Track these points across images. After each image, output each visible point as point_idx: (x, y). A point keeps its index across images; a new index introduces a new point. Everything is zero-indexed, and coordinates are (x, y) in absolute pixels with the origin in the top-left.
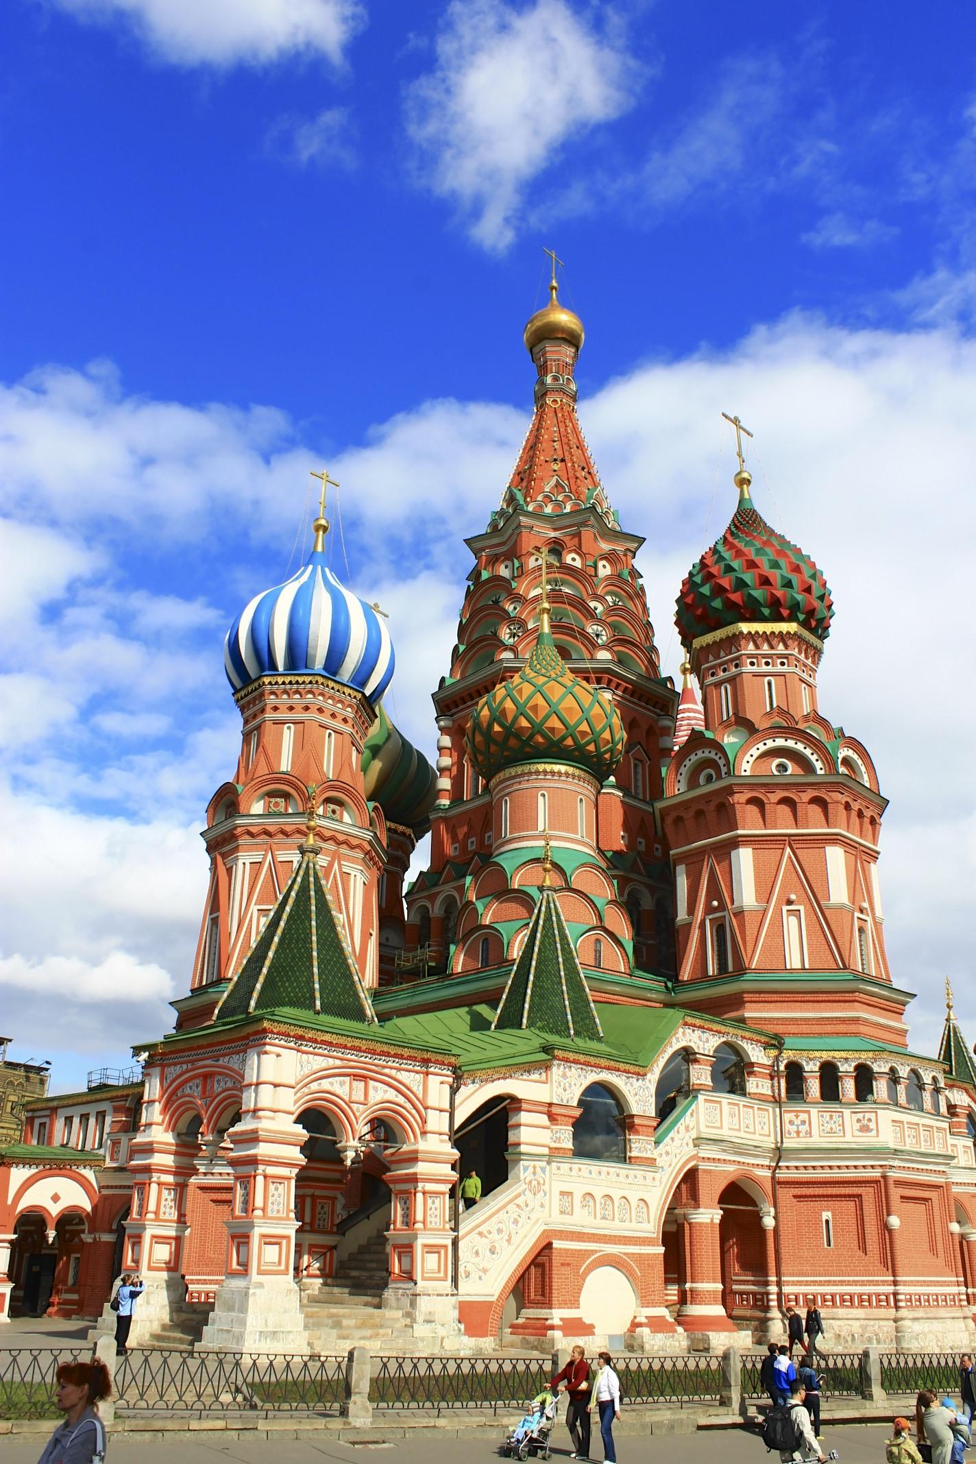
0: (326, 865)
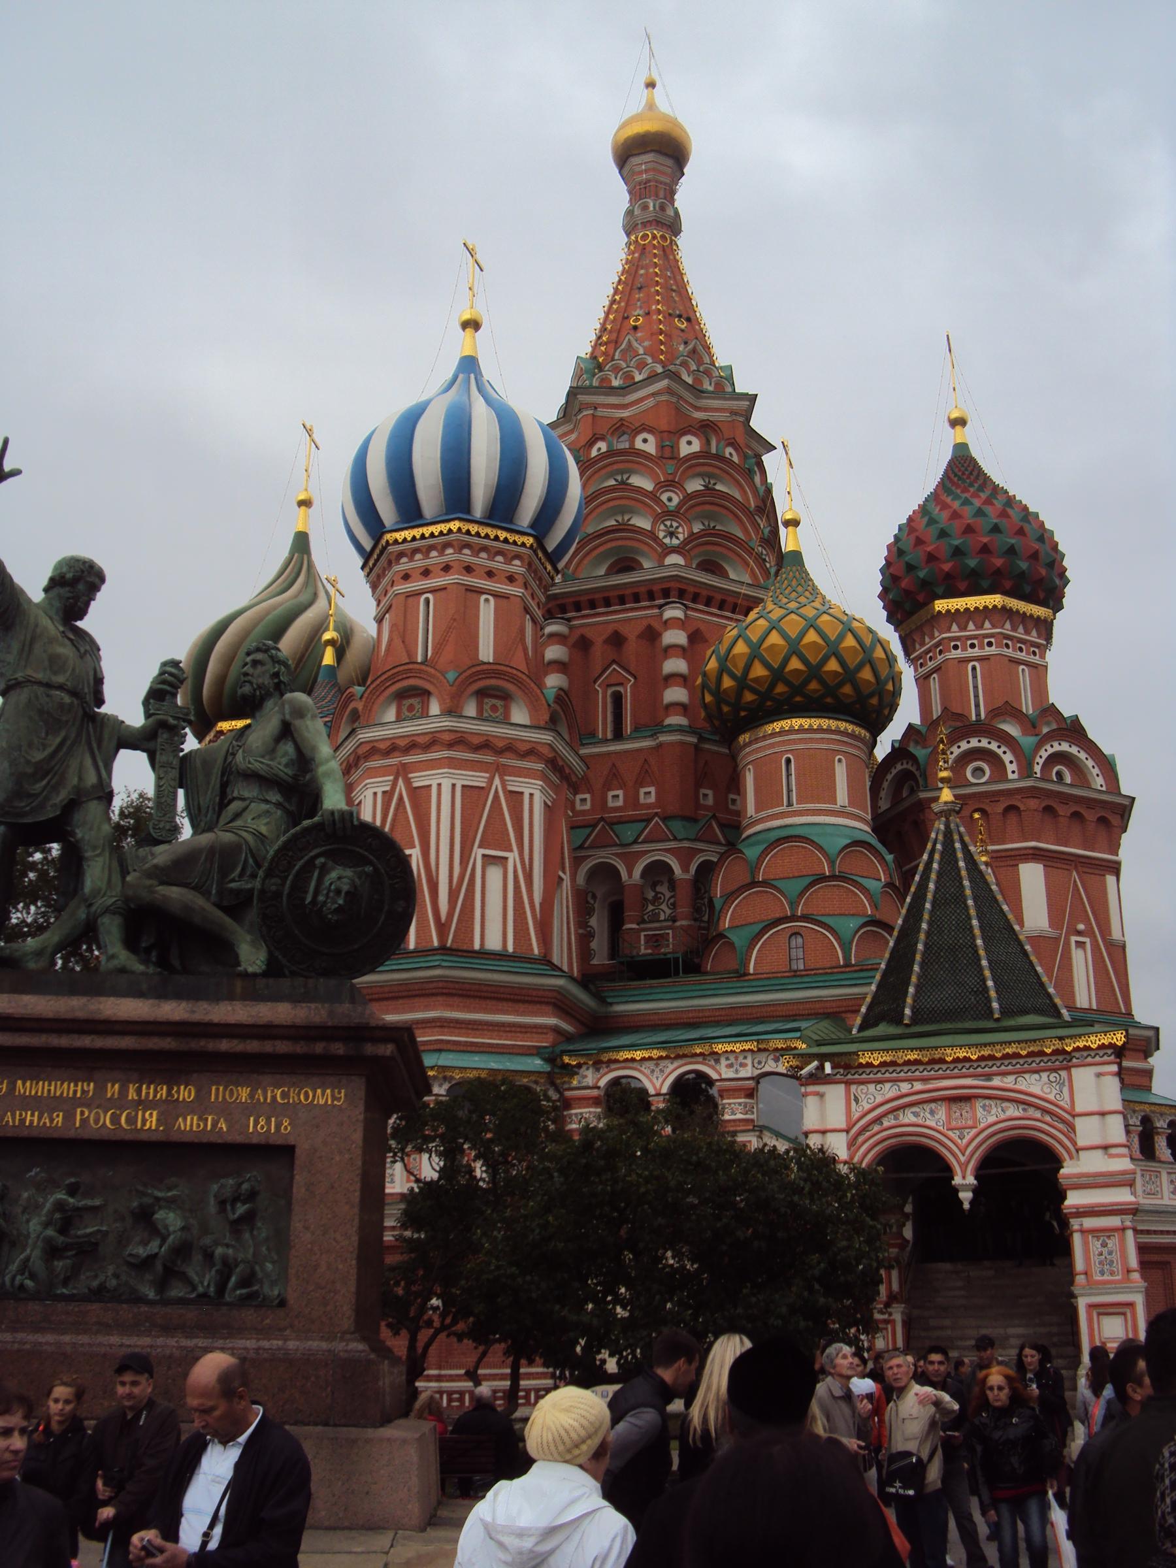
0: (550, 804)
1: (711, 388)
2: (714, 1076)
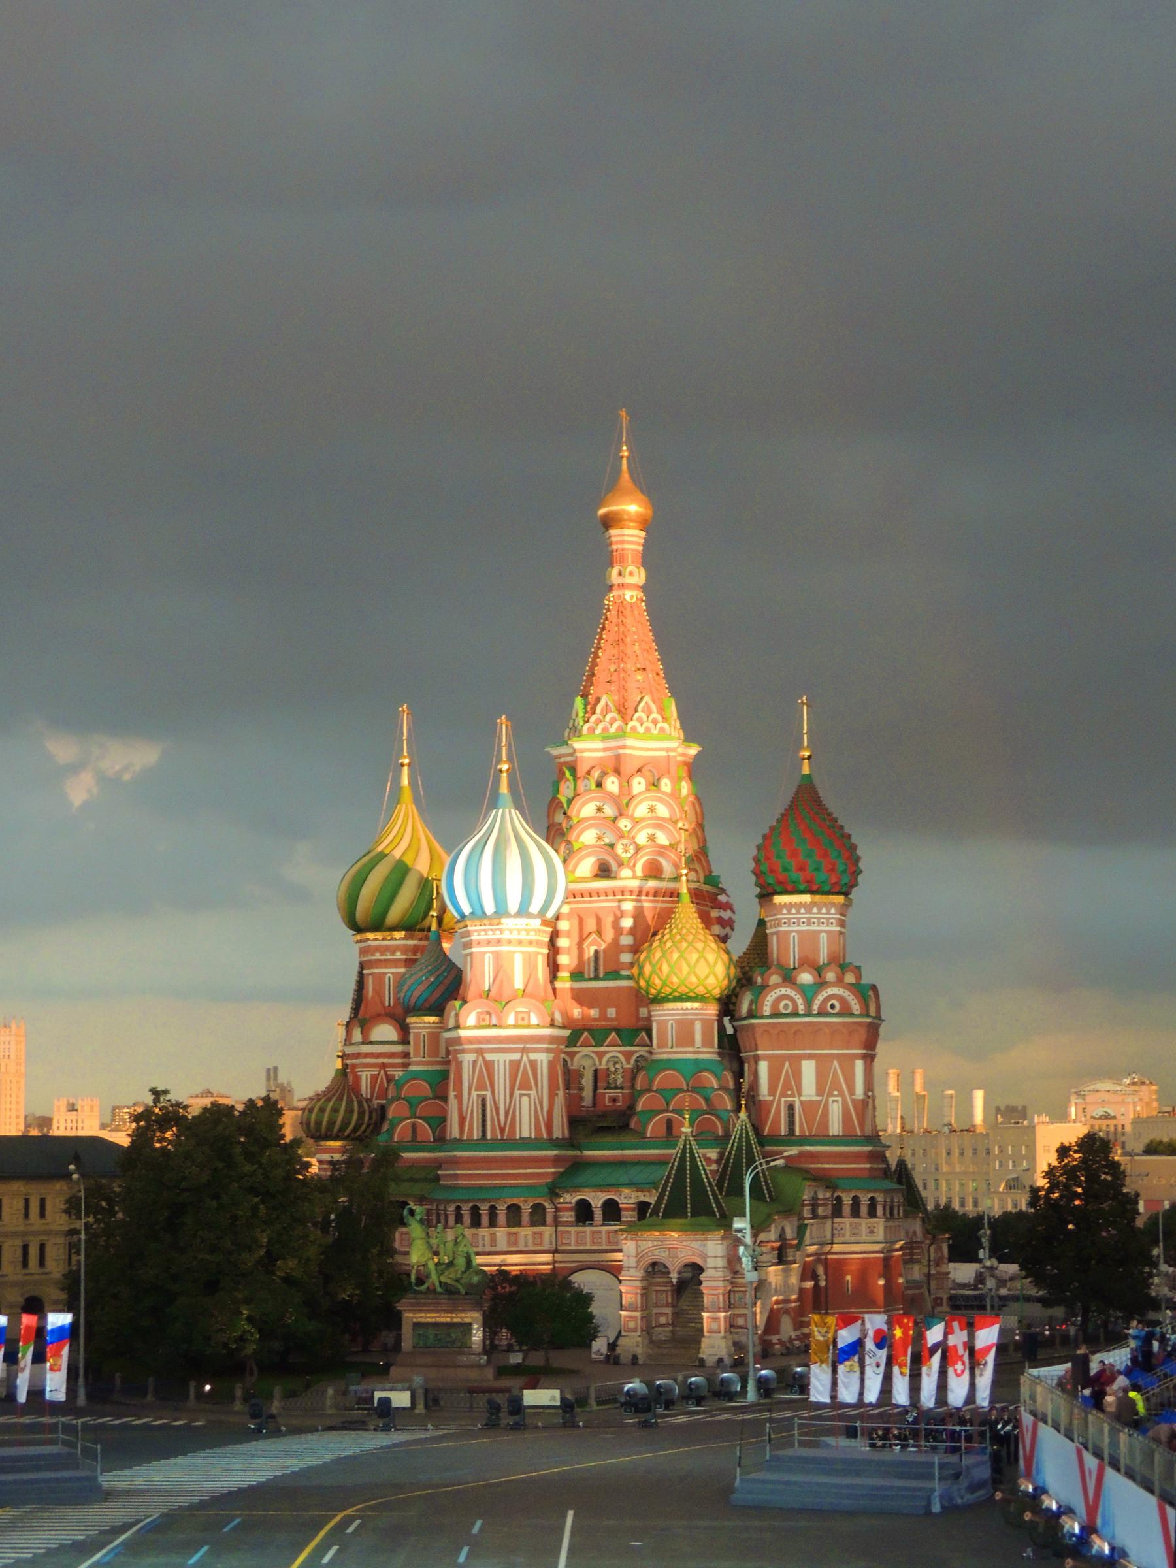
1: (656, 732)
2: (620, 1202)
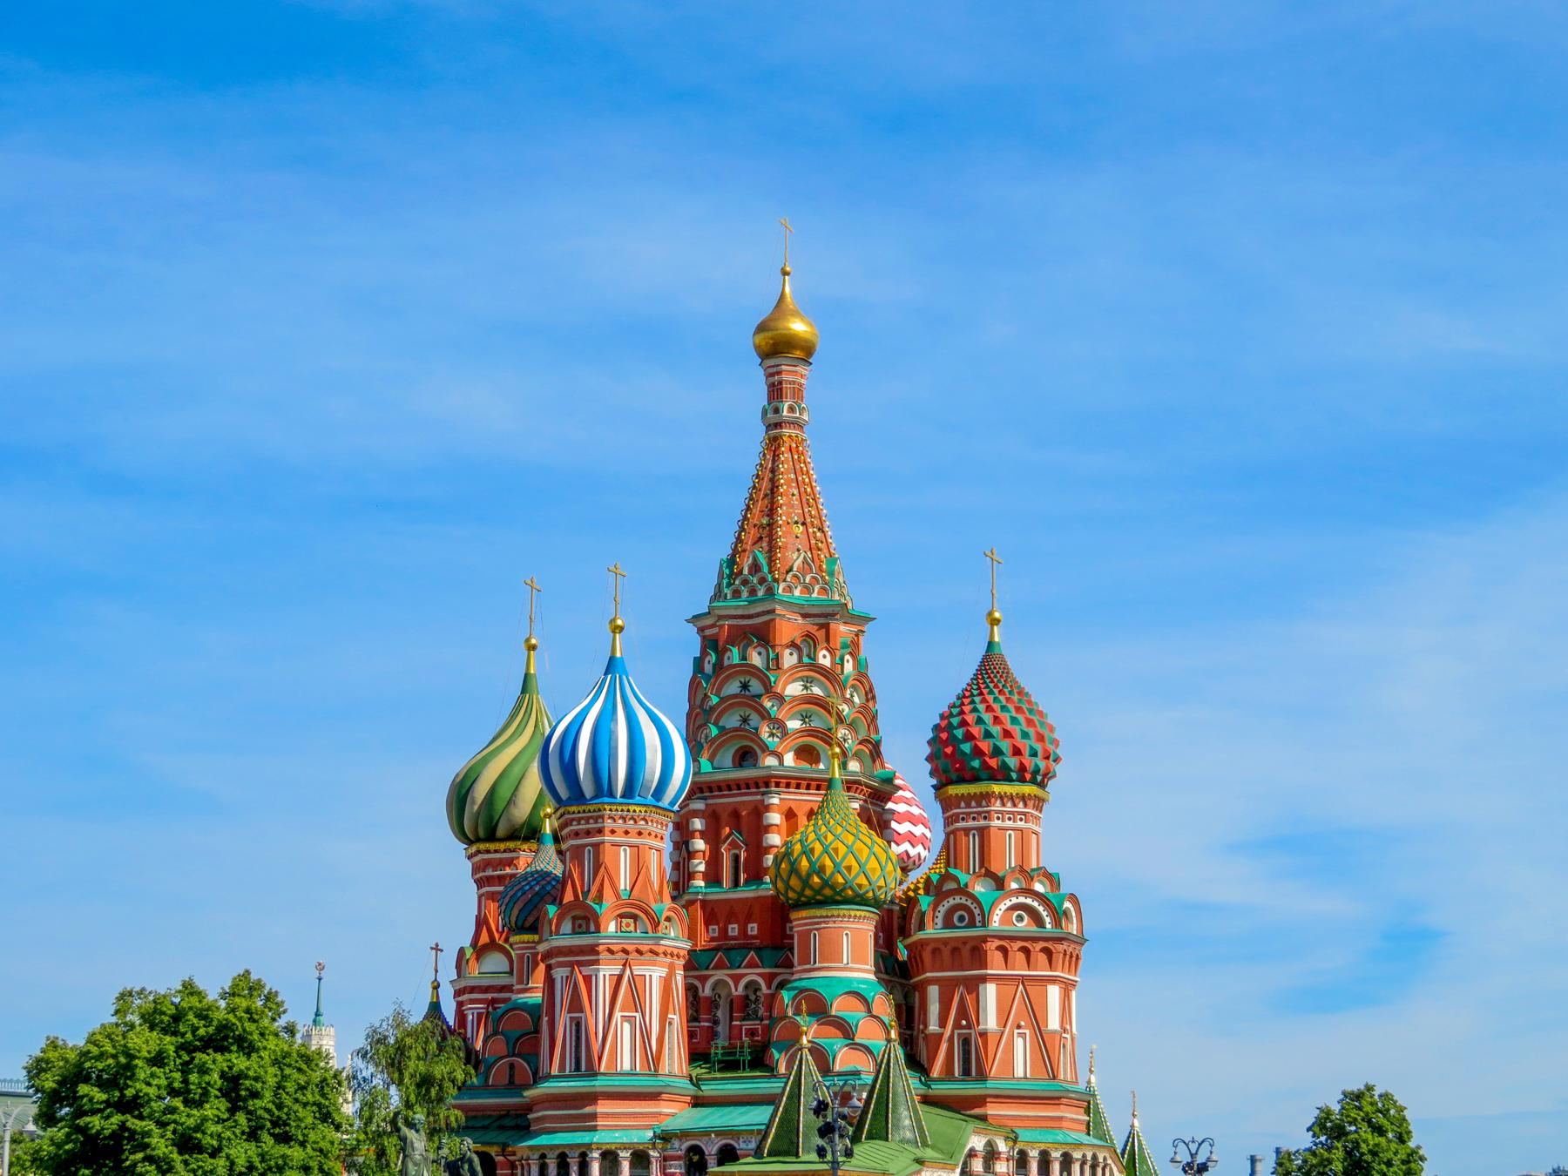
0: (664, 975)
2: (737, 1146)
